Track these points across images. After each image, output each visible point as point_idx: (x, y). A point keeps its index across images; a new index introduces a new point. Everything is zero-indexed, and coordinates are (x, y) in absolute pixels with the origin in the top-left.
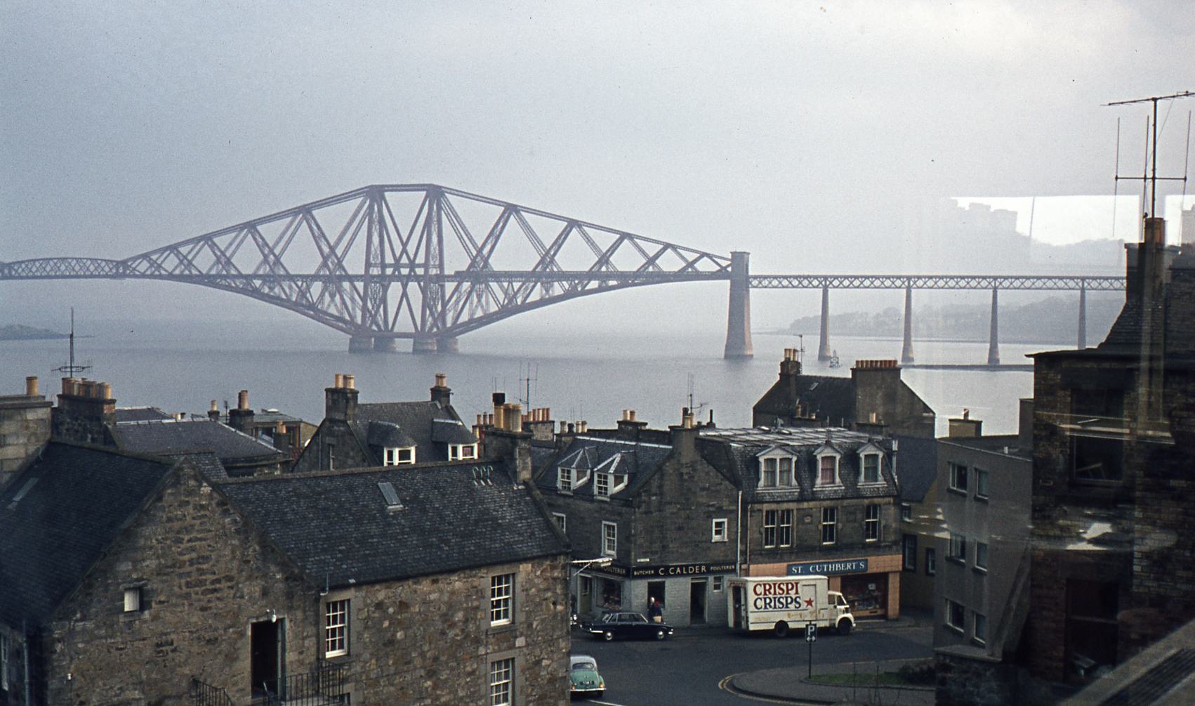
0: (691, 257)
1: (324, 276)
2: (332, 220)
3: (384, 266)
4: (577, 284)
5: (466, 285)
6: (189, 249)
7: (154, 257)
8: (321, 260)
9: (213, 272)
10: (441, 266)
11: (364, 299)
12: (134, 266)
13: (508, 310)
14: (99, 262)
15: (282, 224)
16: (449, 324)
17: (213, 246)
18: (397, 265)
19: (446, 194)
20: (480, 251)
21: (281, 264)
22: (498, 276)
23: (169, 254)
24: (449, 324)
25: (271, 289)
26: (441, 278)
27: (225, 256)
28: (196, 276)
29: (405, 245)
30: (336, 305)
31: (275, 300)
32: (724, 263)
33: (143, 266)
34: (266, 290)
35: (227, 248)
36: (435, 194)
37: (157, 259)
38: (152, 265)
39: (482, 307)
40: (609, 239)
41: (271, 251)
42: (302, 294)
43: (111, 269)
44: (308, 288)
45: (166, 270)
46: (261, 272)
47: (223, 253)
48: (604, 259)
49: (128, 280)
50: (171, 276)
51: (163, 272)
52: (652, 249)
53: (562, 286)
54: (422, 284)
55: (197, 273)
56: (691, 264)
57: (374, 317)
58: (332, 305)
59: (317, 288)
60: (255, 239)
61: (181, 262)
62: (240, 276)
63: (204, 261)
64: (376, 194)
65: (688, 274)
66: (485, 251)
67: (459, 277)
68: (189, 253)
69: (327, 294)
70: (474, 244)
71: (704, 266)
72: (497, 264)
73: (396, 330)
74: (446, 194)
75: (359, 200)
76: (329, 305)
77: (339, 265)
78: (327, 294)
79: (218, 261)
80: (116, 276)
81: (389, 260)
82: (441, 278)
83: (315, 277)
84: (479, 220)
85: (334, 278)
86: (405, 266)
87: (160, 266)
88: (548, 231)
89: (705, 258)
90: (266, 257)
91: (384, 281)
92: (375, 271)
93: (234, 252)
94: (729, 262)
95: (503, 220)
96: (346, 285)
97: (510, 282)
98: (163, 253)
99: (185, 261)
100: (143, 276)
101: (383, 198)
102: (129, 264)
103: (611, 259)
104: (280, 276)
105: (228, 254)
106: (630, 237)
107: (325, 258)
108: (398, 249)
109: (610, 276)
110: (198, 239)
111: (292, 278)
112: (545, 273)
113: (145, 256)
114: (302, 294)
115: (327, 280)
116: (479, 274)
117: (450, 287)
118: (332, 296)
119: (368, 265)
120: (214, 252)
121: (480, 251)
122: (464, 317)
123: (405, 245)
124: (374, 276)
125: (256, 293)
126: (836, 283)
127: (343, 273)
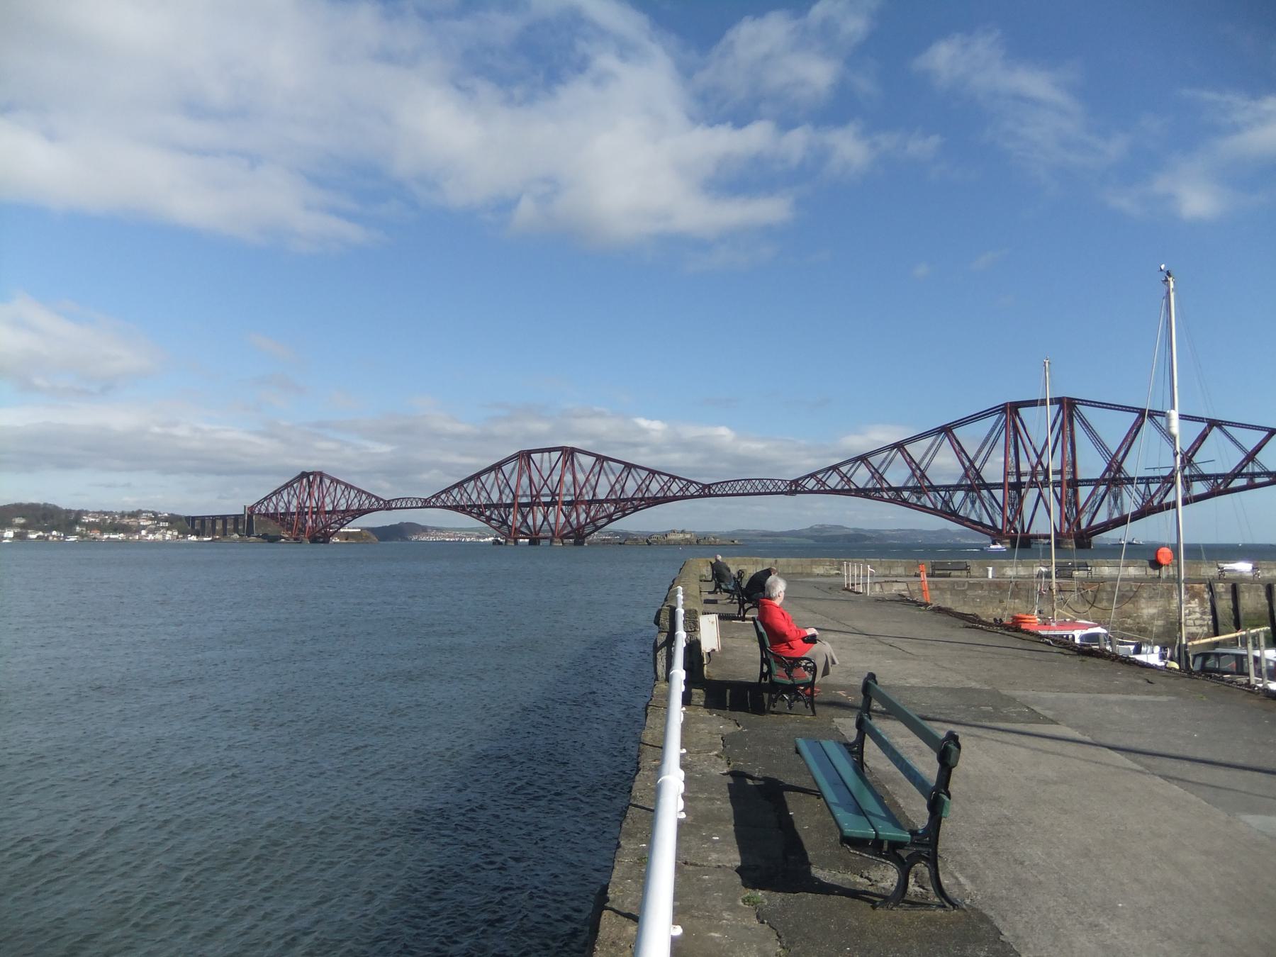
1: (968, 485)
2: (970, 437)
3: (1019, 474)
4: (1221, 486)
5: (1102, 488)
8: (963, 471)
9: (870, 486)
10: (1074, 472)
11: (1003, 509)
12: (803, 484)
13: (1145, 511)
14: (776, 481)
15: (927, 442)
16: (1083, 526)
17: (869, 465)
18: (1034, 473)
23: (832, 473)
24: (1083, 526)
25: (919, 499)
26: (1075, 483)
27: (878, 472)
29: (1039, 457)
30: (976, 511)
31: (923, 508)
33: (811, 484)
34: (913, 499)
35: (881, 465)
36: (1068, 406)
38: (818, 483)
42: (945, 503)
43: (786, 488)
44: (951, 497)
45: (830, 487)
46: (910, 484)
47: (876, 471)
48: (1251, 457)
50: (834, 491)
51: (828, 488)
55: (855, 487)
57: (1011, 523)
58: (973, 512)
59: (959, 496)
60: (904, 456)
61: (842, 479)
62: (890, 488)
63: (862, 476)
64: (1012, 409)
67: (1096, 483)
68: (849, 470)
69: (968, 500)
70: (1107, 450)
73: (1031, 533)
74: (1077, 406)
75: (995, 418)
76: (970, 511)
77: (980, 477)
78: (968, 500)
80: (792, 493)
81: (1025, 467)
82: (1075, 483)
83: (958, 487)
84: (1113, 427)
85: (974, 484)
87: (824, 483)
90: (913, 471)
91: (1018, 486)
92: (1012, 479)
95: (1137, 427)
96: (984, 492)
97: (1147, 484)
98: (827, 472)
99: (877, 476)
100: (811, 492)
101: (1017, 414)
102: (800, 482)
105: (880, 471)
108: (1034, 460)
109: (1259, 475)
111: (936, 489)
113: (812, 475)
115: (969, 489)
116: (1115, 479)
117: (1084, 492)
118: (973, 503)
119: (1006, 474)
120: (869, 470)
122: (1101, 517)
123: (1039, 457)
124: (1010, 484)
125: (905, 503)
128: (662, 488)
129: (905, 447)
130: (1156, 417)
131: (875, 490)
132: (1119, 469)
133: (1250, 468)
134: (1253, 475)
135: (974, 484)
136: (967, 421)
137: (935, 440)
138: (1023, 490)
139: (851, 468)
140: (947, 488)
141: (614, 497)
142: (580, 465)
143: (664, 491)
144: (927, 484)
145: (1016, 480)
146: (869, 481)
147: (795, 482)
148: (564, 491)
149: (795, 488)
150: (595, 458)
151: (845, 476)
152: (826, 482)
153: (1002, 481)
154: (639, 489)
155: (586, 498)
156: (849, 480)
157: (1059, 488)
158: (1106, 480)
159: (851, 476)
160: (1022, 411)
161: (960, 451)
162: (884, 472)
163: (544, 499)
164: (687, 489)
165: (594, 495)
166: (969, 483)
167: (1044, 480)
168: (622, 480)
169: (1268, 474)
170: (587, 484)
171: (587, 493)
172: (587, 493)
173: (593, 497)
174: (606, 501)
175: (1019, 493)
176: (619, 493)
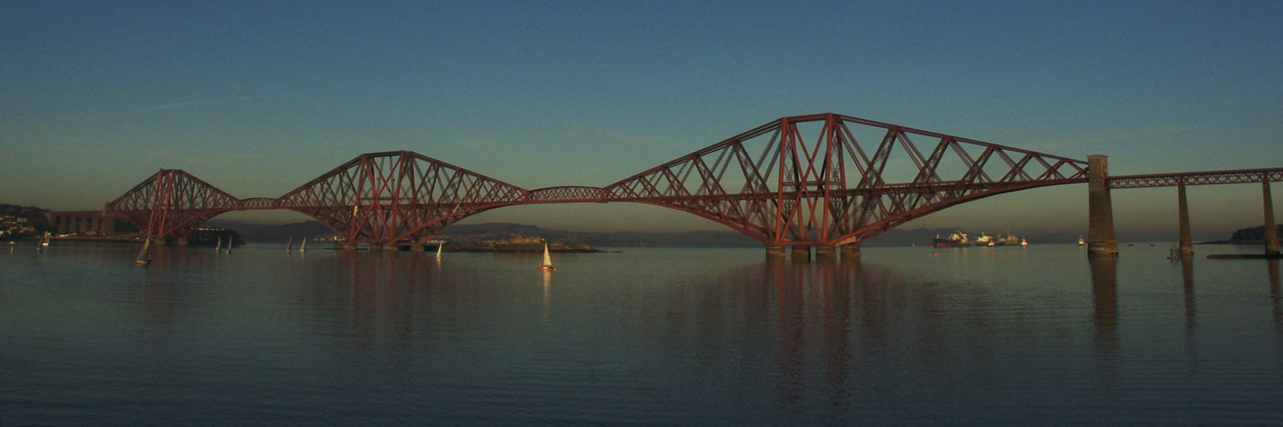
0: (1053, 162)
2: (754, 148)
6: (679, 169)
7: (648, 178)
8: (746, 181)
9: (668, 195)
10: (843, 182)
12: (631, 187)
19: (844, 122)
20: (871, 165)
25: (711, 208)
32: (1083, 167)
33: (619, 192)
36: (835, 122)
37: (651, 180)
38: (625, 191)
39: (876, 216)
41: (711, 175)
43: (597, 196)
44: (739, 204)
45: (636, 194)
46: (702, 194)
48: (976, 169)
49: (610, 203)
50: (639, 199)
52: (1017, 157)
53: (945, 195)
56: (1052, 170)
58: (757, 219)
61: (646, 188)
63: (663, 186)
65: (1051, 179)
66: (877, 166)
67: (854, 193)
71: (1067, 171)
72: (889, 178)
74: (844, 122)
75: (768, 136)
79: (672, 186)
80: (604, 200)
85: (758, 196)
86: (811, 184)
87: (632, 191)
88: (927, 146)
89: (1066, 164)
90: (705, 181)
92: (789, 189)
94: (1087, 166)
100: (619, 199)
103: (983, 169)
104: (718, 196)
105: (680, 179)
106: (999, 148)
107: (749, 180)
109: (982, 185)
111: (726, 197)
112: (925, 185)
113: (621, 184)
114: (734, 209)
116: (872, 191)
121: (871, 165)
124: (788, 193)
126: (1191, 180)
128: (489, 194)
130: (906, 133)
132: (879, 180)
133: (976, 181)
135: (758, 196)
136: (747, 136)
139: (683, 168)
140: (736, 198)
141: (445, 202)
142: (418, 169)
143: (491, 196)
144: (721, 193)
145: (794, 190)
147: (608, 189)
148: (401, 195)
149: (605, 195)
150: (429, 164)
153: (777, 191)
154: (469, 194)
155: (421, 202)
156: (653, 188)
157: (814, 199)
159: (656, 184)
161: (746, 162)
163: (382, 203)
164: (512, 195)
165: (431, 198)
166: (751, 192)
168: (454, 184)
170: (430, 188)
171: (423, 197)
172: (423, 197)
173: (429, 202)
174: (439, 205)
176: (452, 198)
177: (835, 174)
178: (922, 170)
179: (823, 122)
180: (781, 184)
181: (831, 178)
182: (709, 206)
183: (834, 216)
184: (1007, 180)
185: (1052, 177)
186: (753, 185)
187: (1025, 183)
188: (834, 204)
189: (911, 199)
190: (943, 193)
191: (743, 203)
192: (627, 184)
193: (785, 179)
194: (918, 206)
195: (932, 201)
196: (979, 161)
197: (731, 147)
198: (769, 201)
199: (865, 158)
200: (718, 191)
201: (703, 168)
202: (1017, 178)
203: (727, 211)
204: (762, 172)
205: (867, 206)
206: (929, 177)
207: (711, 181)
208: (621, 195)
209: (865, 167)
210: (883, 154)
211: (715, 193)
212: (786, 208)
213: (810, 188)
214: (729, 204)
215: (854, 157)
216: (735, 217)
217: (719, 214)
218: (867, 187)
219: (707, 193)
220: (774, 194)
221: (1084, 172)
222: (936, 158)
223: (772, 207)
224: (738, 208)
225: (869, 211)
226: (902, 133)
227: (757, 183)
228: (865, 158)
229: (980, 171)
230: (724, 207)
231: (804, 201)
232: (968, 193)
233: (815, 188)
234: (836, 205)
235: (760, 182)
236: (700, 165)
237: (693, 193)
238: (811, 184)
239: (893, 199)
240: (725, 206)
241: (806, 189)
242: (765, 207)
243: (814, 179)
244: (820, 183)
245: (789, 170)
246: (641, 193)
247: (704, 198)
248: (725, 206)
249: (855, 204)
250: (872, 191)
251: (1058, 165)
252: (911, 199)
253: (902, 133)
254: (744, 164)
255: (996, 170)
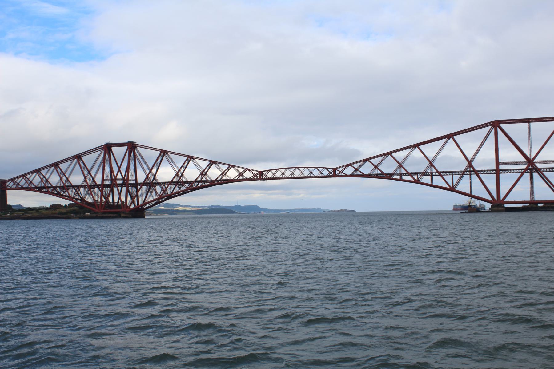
1: (85, 186)
9: (39, 186)
10: (136, 179)
15: (68, 163)
20: (150, 171)
21: (49, 182)
22: (159, 184)
25: (64, 192)
27: (45, 178)
28: (33, 188)
31: (64, 197)
34: (62, 193)
38: (14, 184)
40: (204, 164)
41: (64, 174)
44: (79, 190)
45: (21, 186)
46: (59, 185)
47: (44, 177)
48: (203, 174)
50: (23, 188)
52: (224, 168)
54: (100, 188)
58: (89, 199)
61: (26, 182)
62: (52, 187)
63: (36, 180)
64: (108, 148)
66: (154, 171)
79: (42, 180)
86: (119, 180)
87: (18, 184)
90: (61, 178)
93: (33, 179)
101: (111, 150)
105: (47, 177)
107: (85, 178)
109: (207, 181)
110: (33, 172)
111: (73, 187)
121: (150, 171)
127: (95, 184)
129: (59, 165)
131: (43, 188)
132: (155, 178)
133: (204, 179)
134: (204, 182)
137: (71, 163)
138: (139, 187)
140: (78, 187)
144: (69, 185)
145: (110, 183)
146: (39, 183)
151: (28, 179)
152: (20, 184)
156: (31, 182)
158: (146, 183)
160: (113, 149)
162: (49, 178)
167: (123, 182)
169: (212, 181)
175: (137, 188)
177: (132, 175)
178: (177, 174)
179: (126, 148)
180: (103, 180)
181: (130, 177)
182: (63, 192)
183: (131, 196)
184: (219, 179)
185: (241, 178)
186: (88, 181)
187: (228, 180)
188: (131, 190)
189: (171, 188)
190: (187, 185)
191: (82, 190)
192: (15, 180)
193: (105, 178)
194: (174, 192)
195: (182, 189)
196: (205, 169)
197: (76, 160)
198: (96, 189)
199: (148, 167)
200: (68, 183)
201: (60, 171)
202: (224, 178)
203: (73, 194)
204: (93, 173)
205: (149, 191)
206: (181, 177)
207: (64, 178)
208: (12, 185)
209: (148, 172)
210: (157, 165)
211: (67, 185)
212: (105, 193)
213: (118, 182)
214: (74, 191)
215: (142, 166)
216: (78, 198)
217: (69, 196)
218: (148, 182)
219: (62, 185)
220: (99, 185)
221: (256, 175)
222: (184, 167)
223: (98, 192)
224: (79, 193)
225: (149, 194)
226: (167, 153)
227: (90, 180)
228: (148, 167)
229: (206, 174)
230: (72, 192)
231: (115, 189)
232: (199, 185)
233: (121, 182)
234: (132, 191)
235: (91, 179)
236: (58, 169)
237: (54, 185)
238: (119, 180)
239: (162, 188)
240: (72, 191)
241: (116, 182)
242: (94, 192)
243: (121, 177)
244: (123, 179)
245: (107, 172)
246: (24, 185)
247: (61, 187)
248: (72, 191)
249: (142, 190)
250: (151, 184)
251: (244, 172)
252: (171, 188)
253: (167, 153)
254: (83, 169)
255: (214, 173)
